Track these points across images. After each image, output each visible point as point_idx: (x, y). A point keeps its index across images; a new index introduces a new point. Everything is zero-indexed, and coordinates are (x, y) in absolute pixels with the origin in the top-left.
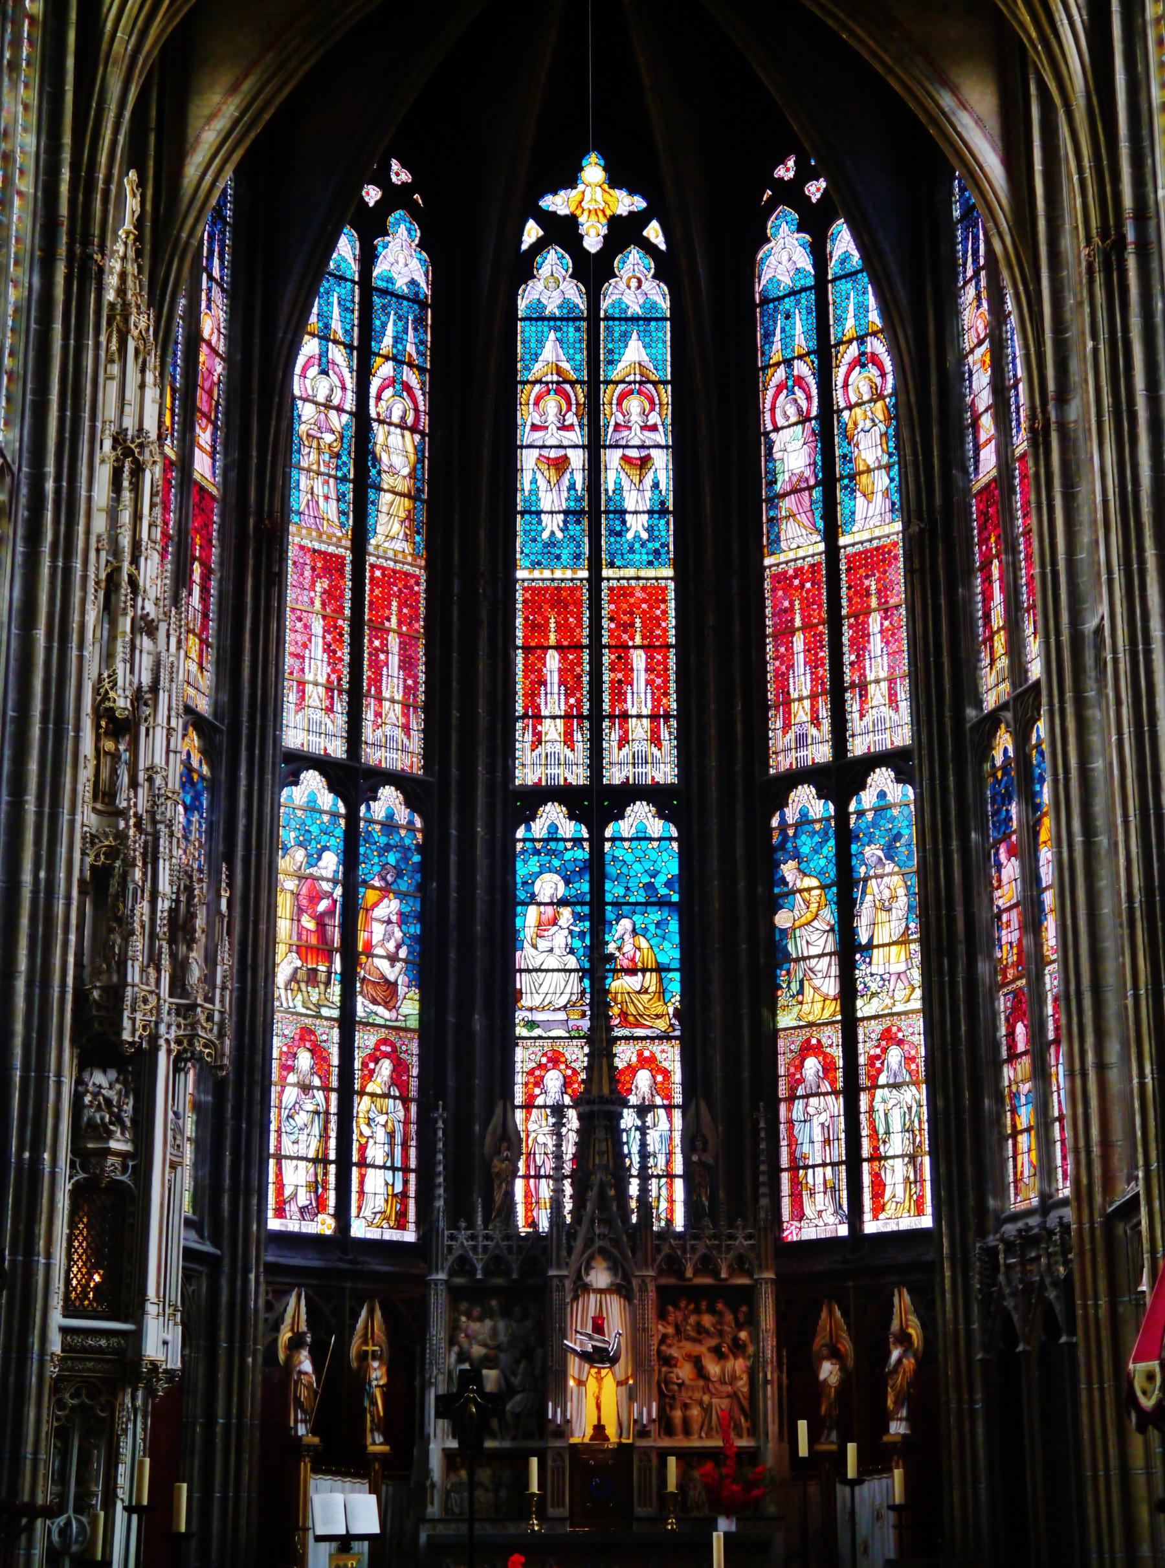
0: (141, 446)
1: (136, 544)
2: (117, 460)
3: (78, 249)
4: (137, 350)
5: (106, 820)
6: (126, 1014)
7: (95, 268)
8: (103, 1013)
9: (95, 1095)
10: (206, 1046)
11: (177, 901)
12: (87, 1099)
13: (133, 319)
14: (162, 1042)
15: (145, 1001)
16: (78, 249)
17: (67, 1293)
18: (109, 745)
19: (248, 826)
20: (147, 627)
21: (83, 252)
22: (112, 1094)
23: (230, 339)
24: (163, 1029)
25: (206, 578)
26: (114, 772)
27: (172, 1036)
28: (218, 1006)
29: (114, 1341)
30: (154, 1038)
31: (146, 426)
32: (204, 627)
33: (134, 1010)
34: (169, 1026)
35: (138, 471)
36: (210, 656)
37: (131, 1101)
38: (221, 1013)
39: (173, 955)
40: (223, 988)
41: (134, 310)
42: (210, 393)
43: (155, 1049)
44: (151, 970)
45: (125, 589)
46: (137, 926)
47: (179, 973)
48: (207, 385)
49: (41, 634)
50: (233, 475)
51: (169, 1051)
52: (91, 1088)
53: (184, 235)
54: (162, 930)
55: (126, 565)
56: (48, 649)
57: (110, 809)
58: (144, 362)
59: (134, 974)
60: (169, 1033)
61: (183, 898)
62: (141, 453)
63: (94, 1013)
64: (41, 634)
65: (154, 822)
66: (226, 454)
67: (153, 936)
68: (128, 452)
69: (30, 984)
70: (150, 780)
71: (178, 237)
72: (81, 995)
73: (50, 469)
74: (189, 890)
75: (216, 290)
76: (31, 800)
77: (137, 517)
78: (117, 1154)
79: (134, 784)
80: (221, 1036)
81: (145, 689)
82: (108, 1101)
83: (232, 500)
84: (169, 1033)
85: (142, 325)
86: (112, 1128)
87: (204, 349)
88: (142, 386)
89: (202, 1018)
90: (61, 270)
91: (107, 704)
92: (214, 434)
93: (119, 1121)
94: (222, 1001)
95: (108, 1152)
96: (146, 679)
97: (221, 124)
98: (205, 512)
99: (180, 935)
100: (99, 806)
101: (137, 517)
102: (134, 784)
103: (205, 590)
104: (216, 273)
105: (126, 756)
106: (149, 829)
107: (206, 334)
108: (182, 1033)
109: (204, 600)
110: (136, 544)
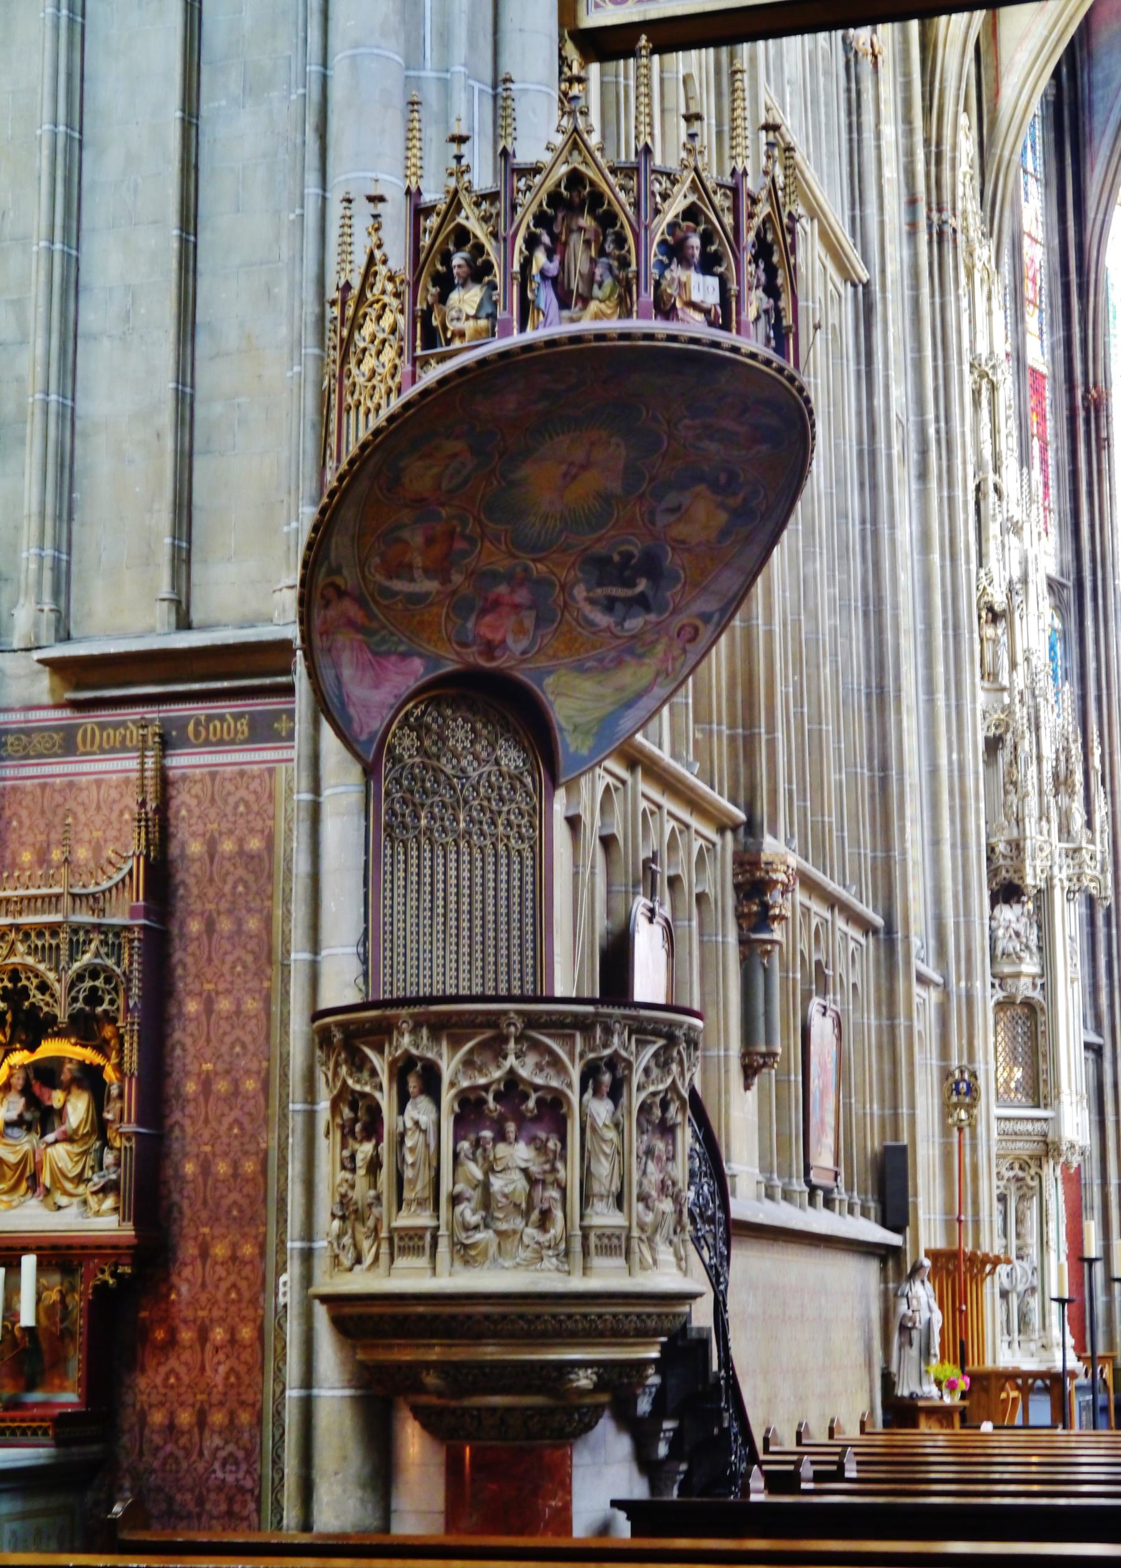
0: (994, 367)
1: (996, 456)
2: (975, 382)
3: (935, 216)
4: (982, 280)
5: (993, 695)
6: (1028, 862)
7: (950, 231)
8: (1008, 862)
9: (1007, 928)
10: (1091, 880)
11: (1057, 759)
12: (1000, 932)
13: (976, 254)
14: (1056, 882)
15: (1041, 850)
16: (935, 216)
17: (997, 1090)
18: (989, 631)
19: (1098, 669)
20: (1016, 529)
21: (940, 218)
22: (1020, 927)
23: (1046, 225)
24: (1056, 869)
25: (1043, 450)
26: (995, 654)
27: (1064, 876)
28: (1099, 847)
29: (1038, 1126)
30: (1050, 880)
31: (996, 351)
32: (1046, 495)
33: (1033, 859)
34: (1061, 868)
35: (993, 388)
36: (1053, 519)
37: (1035, 930)
38: (1102, 853)
39: (1059, 809)
40: (1102, 832)
41: (977, 245)
42: (1034, 281)
43: (1050, 887)
44: (1044, 823)
45: (992, 496)
46: (1030, 788)
47: (1064, 821)
48: (1031, 274)
49: (936, 557)
50: (1060, 352)
51: (1063, 889)
52: (1002, 923)
53: (1006, 154)
54: (1048, 787)
55: (991, 478)
56: (943, 567)
57: (996, 686)
58: (990, 292)
59: (1031, 826)
60: (1061, 875)
61: (1062, 758)
62: (994, 374)
63: (1001, 862)
64: (936, 557)
65: (1034, 696)
66: (1052, 334)
67: (1041, 793)
68: (983, 375)
69: (953, 846)
70: (1027, 659)
71: (1001, 157)
72: (991, 849)
73: (931, 416)
74: (1067, 750)
75: (1031, 181)
76: (940, 696)
77: (994, 432)
78: (1028, 975)
79: (1013, 665)
80: (1103, 871)
81: (1015, 579)
82: (1017, 934)
83: (1061, 375)
84: (1061, 875)
85: (985, 258)
86: (1022, 954)
87: (1026, 241)
88: (990, 313)
89: (1088, 858)
90: (923, 237)
91: (986, 598)
92: (1040, 317)
93: (1027, 947)
94: (1102, 842)
95: (1018, 975)
96: (1016, 574)
97: (1032, 44)
98: (1038, 392)
99: (1062, 789)
100: (986, 685)
101: (994, 432)
102: (1013, 665)
103: (1044, 461)
104: (1030, 168)
105: (1004, 639)
106: (1031, 703)
107: (1026, 228)
108: (1071, 871)
109: (1044, 471)
110: (996, 456)
